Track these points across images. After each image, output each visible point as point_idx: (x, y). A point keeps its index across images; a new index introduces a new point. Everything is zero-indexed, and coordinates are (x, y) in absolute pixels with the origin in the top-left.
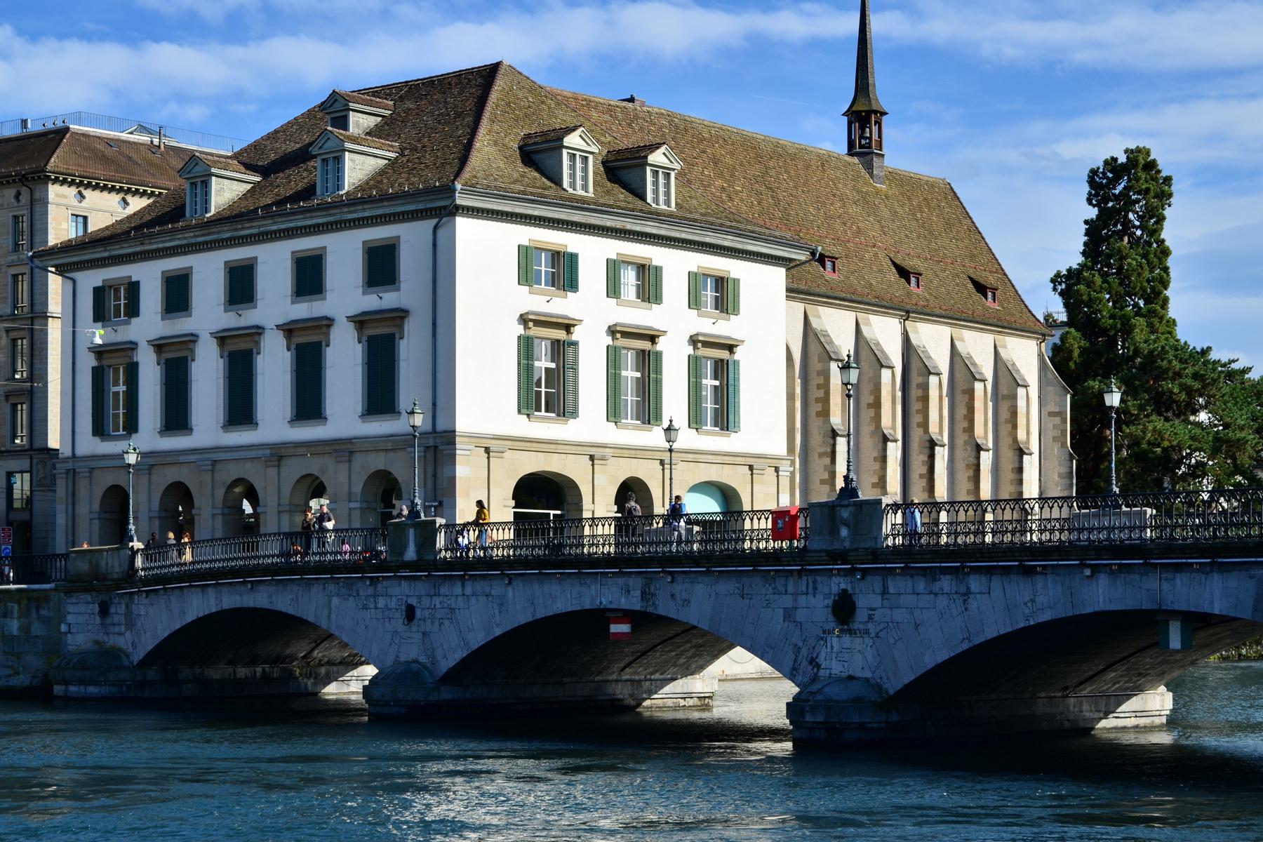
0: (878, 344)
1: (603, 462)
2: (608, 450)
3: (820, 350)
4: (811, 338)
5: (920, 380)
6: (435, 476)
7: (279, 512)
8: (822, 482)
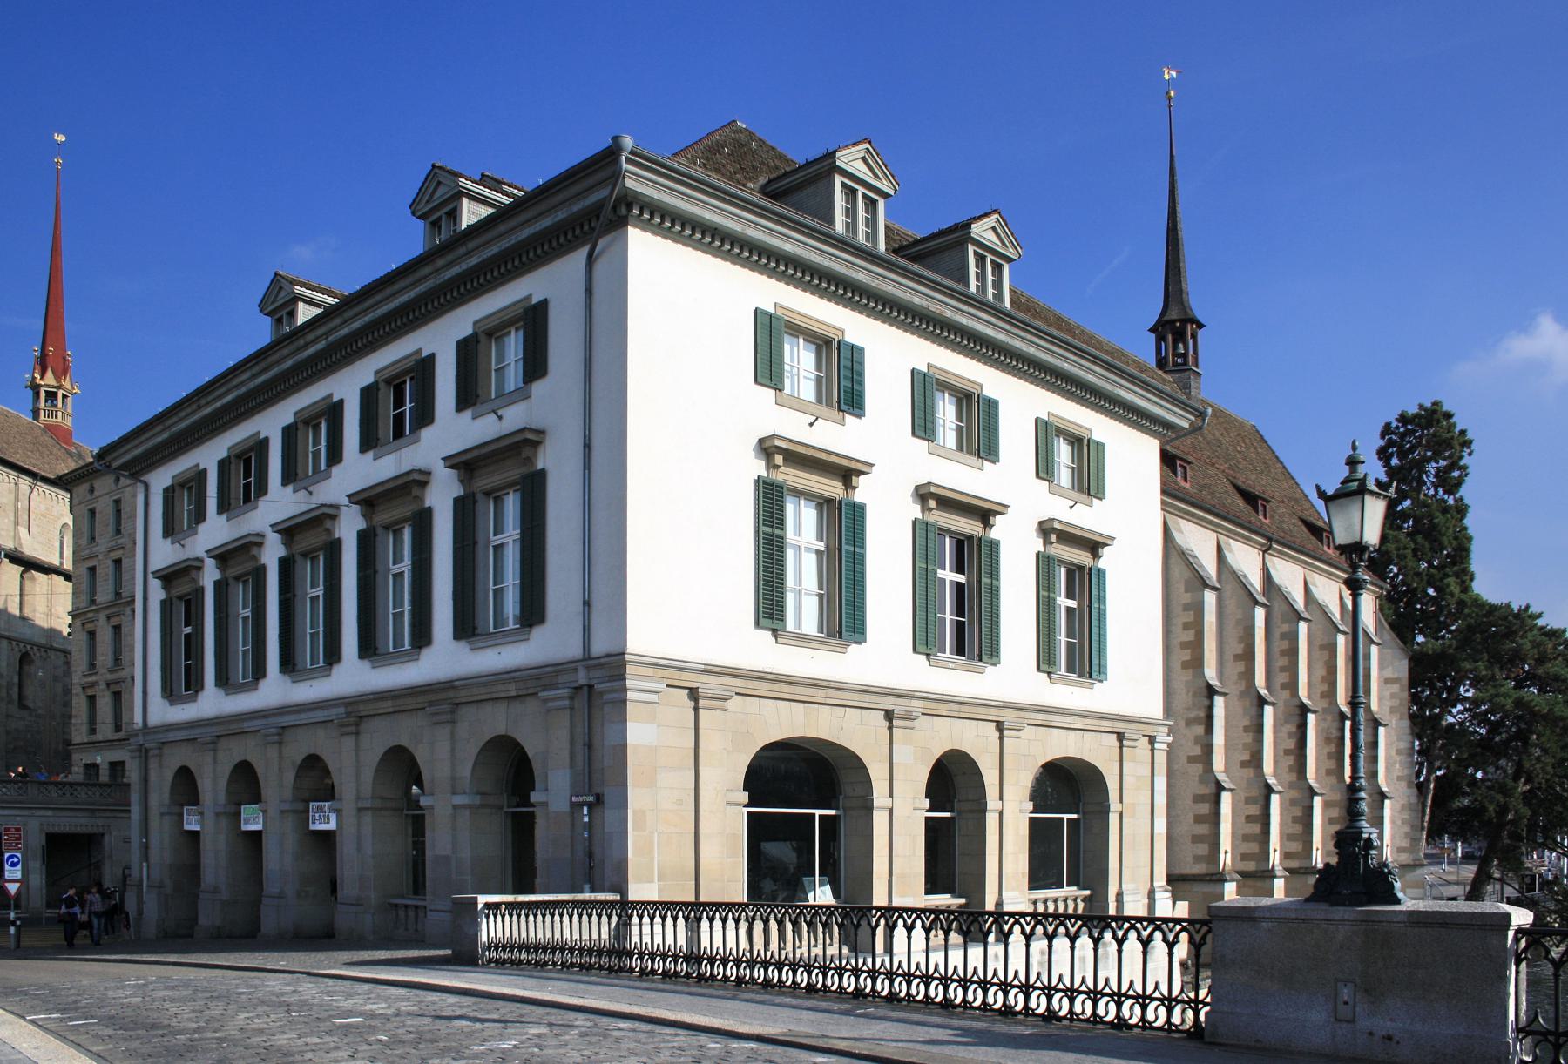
0: (1245, 576)
1: (907, 723)
2: (915, 703)
3: (1187, 574)
4: (1174, 559)
5: (1285, 628)
6: (589, 746)
7: (360, 810)
8: (1192, 760)
